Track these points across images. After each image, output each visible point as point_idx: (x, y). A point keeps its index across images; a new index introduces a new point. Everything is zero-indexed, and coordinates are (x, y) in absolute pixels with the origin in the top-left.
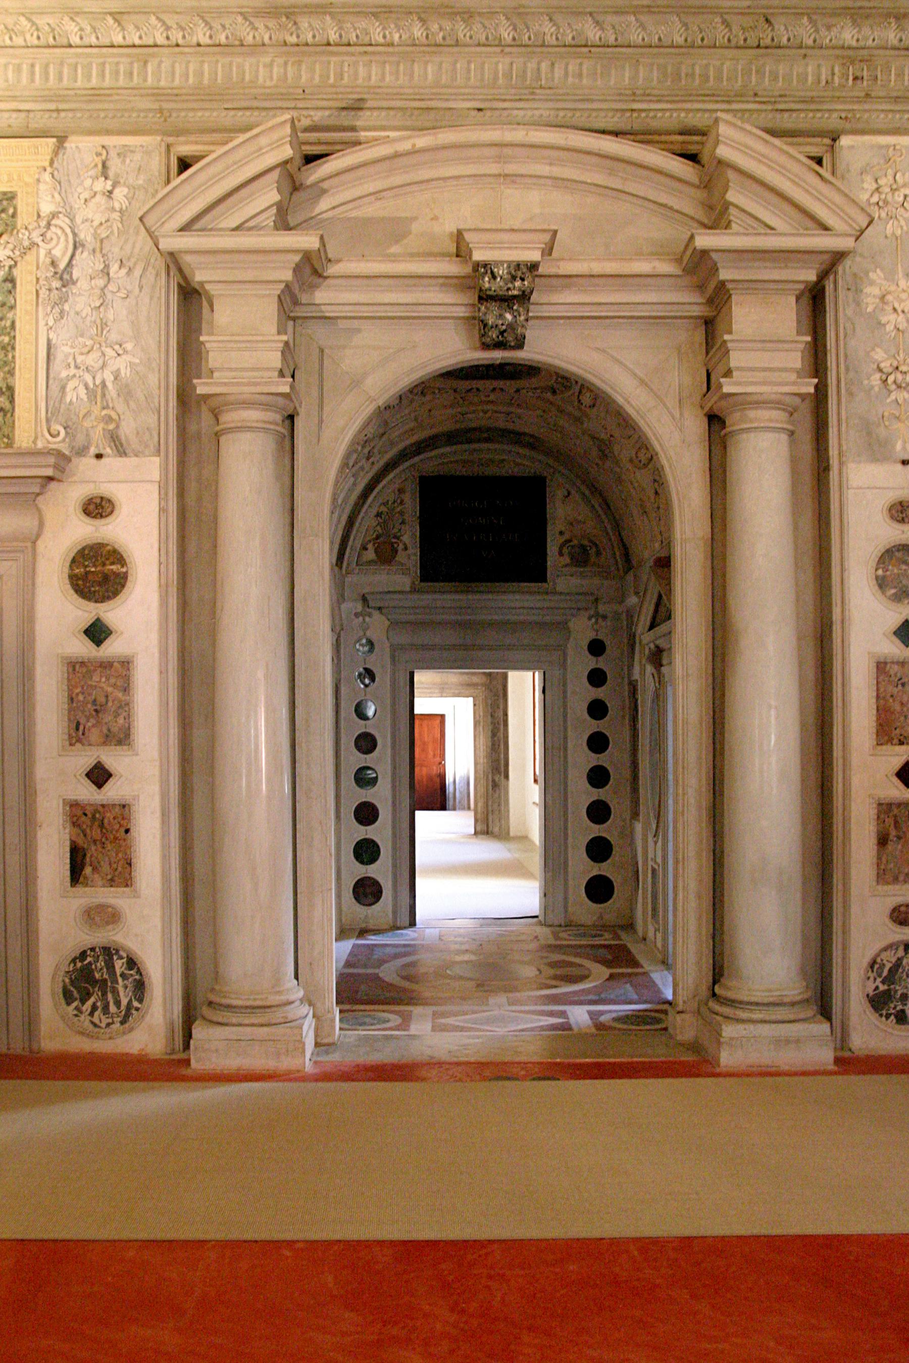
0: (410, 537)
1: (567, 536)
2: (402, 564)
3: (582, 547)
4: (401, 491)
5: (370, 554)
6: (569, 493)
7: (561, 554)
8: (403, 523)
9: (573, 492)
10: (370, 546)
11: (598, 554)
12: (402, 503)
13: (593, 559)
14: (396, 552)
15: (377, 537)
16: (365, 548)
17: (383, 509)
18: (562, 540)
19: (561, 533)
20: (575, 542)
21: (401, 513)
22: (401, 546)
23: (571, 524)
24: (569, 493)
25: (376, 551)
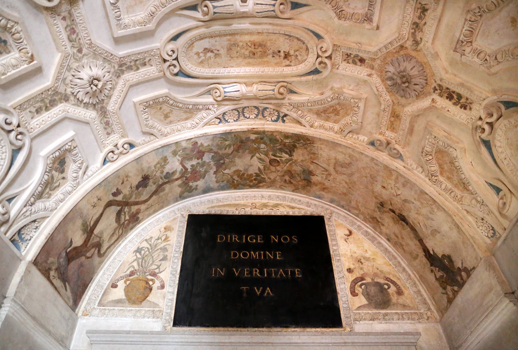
0: (170, 274)
1: (357, 274)
2: (156, 305)
3: (380, 286)
4: (167, 229)
5: (119, 293)
6: (351, 233)
7: (354, 294)
8: (165, 258)
9: (354, 231)
10: (121, 285)
11: (400, 292)
12: (166, 239)
13: (394, 298)
14: (151, 289)
15: (132, 274)
16: (114, 286)
17: (145, 245)
18: (351, 277)
19: (350, 271)
20: (368, 280)
21: (164, 249)
22: (157, 284)
23: (359, 261)
24: (351, 233)
25: (127, 290)
